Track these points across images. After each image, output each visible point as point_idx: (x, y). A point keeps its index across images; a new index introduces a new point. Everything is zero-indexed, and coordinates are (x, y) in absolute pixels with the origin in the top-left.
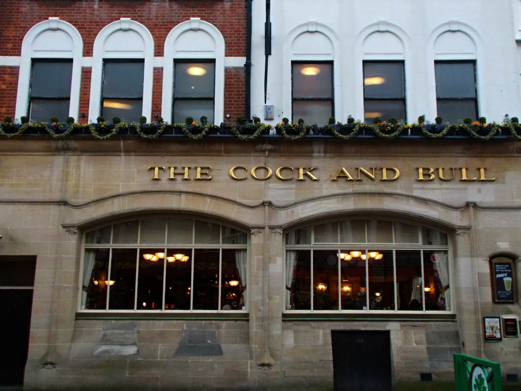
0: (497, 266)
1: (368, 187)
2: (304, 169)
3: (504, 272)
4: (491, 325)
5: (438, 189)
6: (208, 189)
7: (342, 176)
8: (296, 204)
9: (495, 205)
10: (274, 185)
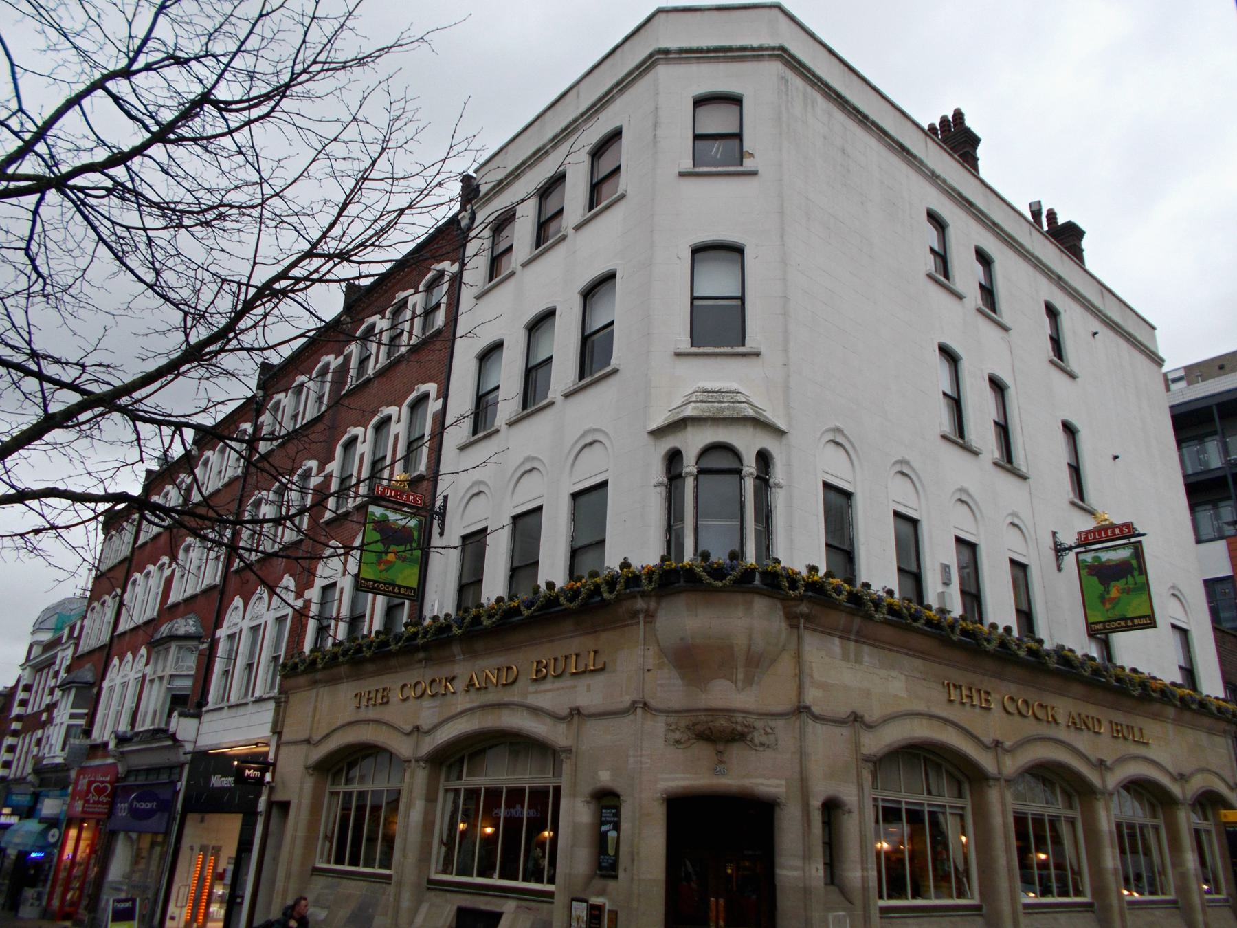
1: (491, 697)
2: (446, 679)
3: (609, 822)
4: (578, 913)
6: (386, 714)
7: (471, 684)
8: (435, 728)
9: (601, 709)
10: (426, 703)
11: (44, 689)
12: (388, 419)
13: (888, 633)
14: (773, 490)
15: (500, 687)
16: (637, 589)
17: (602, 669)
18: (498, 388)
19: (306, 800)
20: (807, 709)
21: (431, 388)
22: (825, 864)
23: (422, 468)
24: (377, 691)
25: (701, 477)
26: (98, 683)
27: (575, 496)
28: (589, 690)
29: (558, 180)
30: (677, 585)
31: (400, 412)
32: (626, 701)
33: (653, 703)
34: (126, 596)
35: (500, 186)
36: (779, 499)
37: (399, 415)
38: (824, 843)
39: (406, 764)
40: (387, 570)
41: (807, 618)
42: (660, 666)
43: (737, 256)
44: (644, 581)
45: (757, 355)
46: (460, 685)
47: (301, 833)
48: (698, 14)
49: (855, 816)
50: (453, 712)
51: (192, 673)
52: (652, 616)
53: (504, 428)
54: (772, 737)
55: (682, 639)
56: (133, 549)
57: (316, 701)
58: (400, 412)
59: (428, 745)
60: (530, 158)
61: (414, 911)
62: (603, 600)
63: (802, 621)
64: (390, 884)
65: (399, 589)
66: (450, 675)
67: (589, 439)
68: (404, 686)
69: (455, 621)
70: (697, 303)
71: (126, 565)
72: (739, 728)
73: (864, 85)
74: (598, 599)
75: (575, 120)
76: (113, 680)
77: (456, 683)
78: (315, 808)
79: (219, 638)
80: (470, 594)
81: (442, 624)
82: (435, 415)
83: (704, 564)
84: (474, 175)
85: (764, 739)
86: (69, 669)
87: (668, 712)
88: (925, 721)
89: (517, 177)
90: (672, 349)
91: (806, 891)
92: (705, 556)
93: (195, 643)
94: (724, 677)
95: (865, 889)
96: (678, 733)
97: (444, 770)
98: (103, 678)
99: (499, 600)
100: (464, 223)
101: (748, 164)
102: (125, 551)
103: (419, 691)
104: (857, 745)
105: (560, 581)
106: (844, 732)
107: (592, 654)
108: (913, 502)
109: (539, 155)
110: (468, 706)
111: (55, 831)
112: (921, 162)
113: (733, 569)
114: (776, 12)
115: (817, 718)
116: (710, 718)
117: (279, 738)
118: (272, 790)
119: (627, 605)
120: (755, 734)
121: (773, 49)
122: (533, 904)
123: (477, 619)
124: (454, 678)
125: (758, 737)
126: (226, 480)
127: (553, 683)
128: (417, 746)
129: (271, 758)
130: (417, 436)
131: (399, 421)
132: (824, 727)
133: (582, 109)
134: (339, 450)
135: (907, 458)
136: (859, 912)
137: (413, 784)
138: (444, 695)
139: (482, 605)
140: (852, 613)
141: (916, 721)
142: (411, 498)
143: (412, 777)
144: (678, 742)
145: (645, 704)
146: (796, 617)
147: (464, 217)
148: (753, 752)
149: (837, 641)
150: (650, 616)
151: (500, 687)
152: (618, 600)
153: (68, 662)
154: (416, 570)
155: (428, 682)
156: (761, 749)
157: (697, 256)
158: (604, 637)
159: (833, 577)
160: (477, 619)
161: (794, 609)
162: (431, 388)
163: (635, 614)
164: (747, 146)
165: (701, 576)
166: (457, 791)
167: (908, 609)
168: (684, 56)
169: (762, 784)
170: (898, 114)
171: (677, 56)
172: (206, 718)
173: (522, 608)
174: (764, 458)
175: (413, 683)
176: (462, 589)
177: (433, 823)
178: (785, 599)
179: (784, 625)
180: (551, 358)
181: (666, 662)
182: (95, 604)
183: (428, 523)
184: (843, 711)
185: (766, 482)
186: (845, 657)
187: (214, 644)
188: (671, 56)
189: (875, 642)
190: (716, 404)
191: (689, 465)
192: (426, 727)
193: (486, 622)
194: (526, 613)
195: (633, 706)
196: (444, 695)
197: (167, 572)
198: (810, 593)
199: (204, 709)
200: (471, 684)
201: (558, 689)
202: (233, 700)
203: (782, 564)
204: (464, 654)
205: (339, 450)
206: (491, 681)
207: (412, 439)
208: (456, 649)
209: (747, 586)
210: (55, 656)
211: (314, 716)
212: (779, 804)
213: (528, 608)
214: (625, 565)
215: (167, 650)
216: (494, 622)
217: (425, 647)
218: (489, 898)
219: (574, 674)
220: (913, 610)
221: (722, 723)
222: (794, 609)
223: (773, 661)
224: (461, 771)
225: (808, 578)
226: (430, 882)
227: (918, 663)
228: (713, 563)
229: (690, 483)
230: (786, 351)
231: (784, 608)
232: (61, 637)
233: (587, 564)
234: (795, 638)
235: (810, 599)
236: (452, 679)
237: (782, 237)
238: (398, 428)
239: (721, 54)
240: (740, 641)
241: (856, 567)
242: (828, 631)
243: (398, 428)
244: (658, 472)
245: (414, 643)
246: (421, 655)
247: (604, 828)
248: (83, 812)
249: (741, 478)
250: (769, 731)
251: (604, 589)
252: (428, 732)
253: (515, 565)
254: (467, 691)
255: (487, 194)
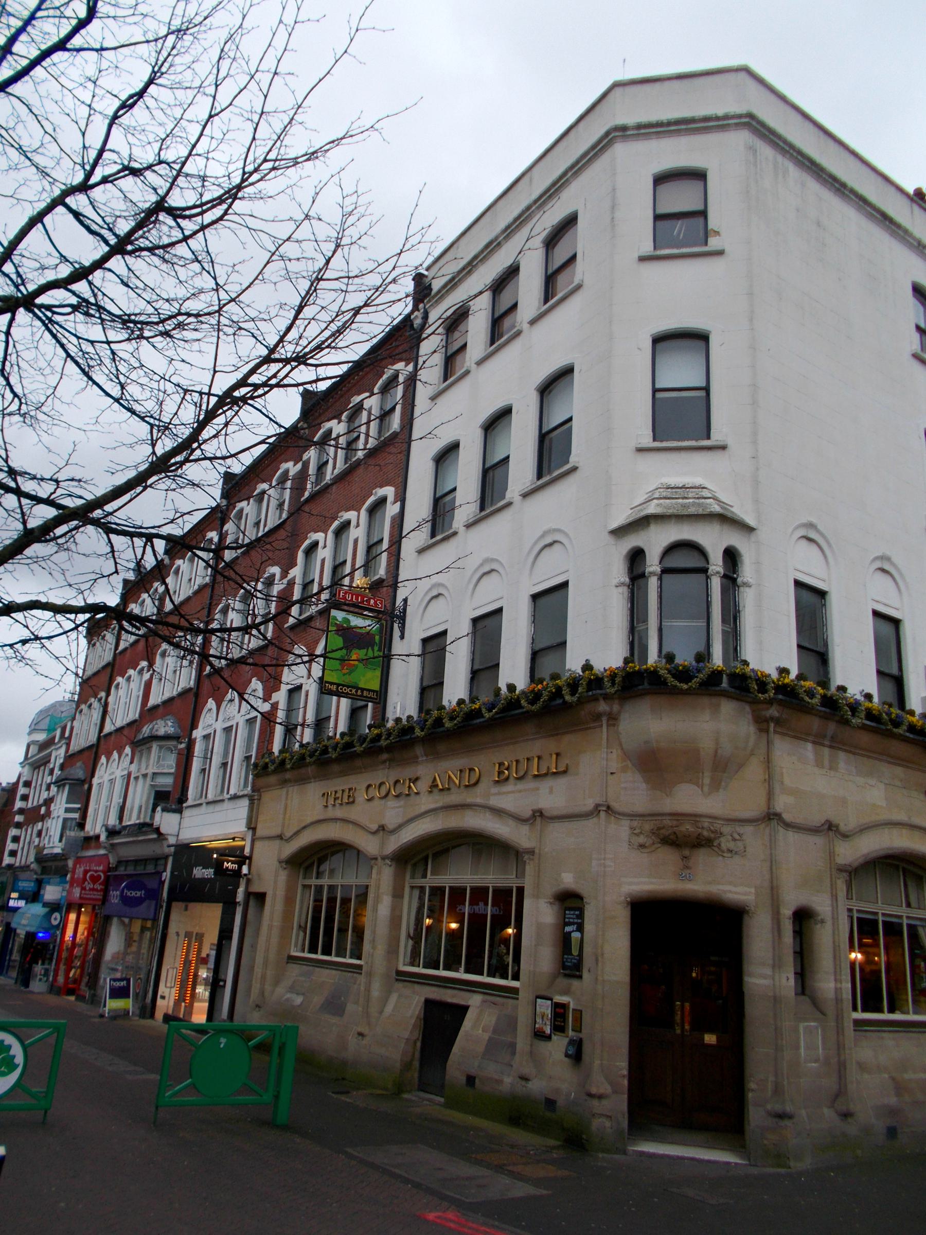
0: (567, 912)
1: (454, 798)
2: (410, 780)
3: (573, 924)
4: (542, 1010)
5: (513, 792)
6: (353, 813)
8: (400, 827)
10: (391, 803)
11: (41, 785)
12: (348, 523)
13: (865, 738)
14: (742, 589)
15: (462, 787)
16: (599, 692)
17: (565, 772)
18: (454, 489)
19: (281, 892)
20: (778, 816)
21: (389, 491)
22: (796, 973)
23: (382, 572)
24: (343, 791)
25: (665, 576)
26: (88, 779)
27: (535, 597)
28: (551, 792)
29: (513, 271)
30: (640, 687)
31: (326, 538)
32: (589, 804)
33: (615, 805)
34: (111, 699)
35: (453, 283)
36: (748, 599)
37: (325, 541)
38: (795, 952)
39: (373, 862)
40: (349, 674)
41: (778, 722)
42: (624, 770)
43: (702, 344)
44: (607, 684)
45: (723, 448)
46: (423, 785)
47: (277, 923)
48: (657, 85)
49: (829, 926)
50: (417, 812)
51: (173, 771)
52: (615, 719)
53: (462, 530)
54: (740, 844)
55: (646, 742)
56: (115, 654)
57: (287, 799)
58: (326, 538)
59: (394, 844)
60: (482, 251)
61: (384, 1001)
62: (565, 702)
63: (772, 725)
64: (361, 974)
65: (362, 692)
66: (413, 776)
67: (548, 540)
68: (369, 786)
69: (418, 722)
70: (659, 395)
71: (109, 669)
72: (705, 833)
73: (841, 149)
74: (560, 701)
75: (528, 208)
76: (101, 777)
77: (419, 783)
78: (289, 900)
79: (195, 739)
80: (430, 695)
81: (404, 726)
82: (393, 519)
83: (668, 666)
84: (426, 273)
85: (731, 845)
86: (62, 767)
87: (632, 816)
88: (904, 831)
89: (470, 273)
90: (633, 444)
91: (776, 1000)
92: (670, 658)
93: (174, 743)
94: (690, 781)
95: (838, 1000)
96: (642, 836)
97: (409, 868)
98: (93, 775)
99: (461, 702)
100: (417, 322)
101: (714, 243)
102: (108, 657)
103: (384, 791)
104: (832, 855)
105: (522, 683)
106: (817, 842)
107: (554, 756)
108: (895, 602)
109: (492, 247)
110: (432, 806)
111: (57, 915)
112: (906, 231)
113: (699, 671)
114: (743, 75)
115: (788, 825)
116: (675, 823)
117: (254, 834)
118: (249, 882)
119: (589, 707)
120: (723, 840)
121: (740, 116)
122: (498, 999)
123: (439, 722)
124: (417, 779)
125: (725, 843)
126: (196, 587)
127: (516, 784)
128: (383, 844)
129: (247, 851)
130: (376, 540)
131: (358, 525)
132: (797, 836)
133: (535, 196)
134: (300, 556)
135: (888, 553)
136: (833, 1024)
137: (379, 880)
138: (408, 795)
139: (443, 708)
140: (825, 717)
141: (895, 832)
142: (372, 602)
143: (379, 873)
144: (642, 846)
145: (609, 807)
146: (767, 720)
147: (416, 316)
148: (721, 858)
149: (809, 746)
150: (613, 719)
151: (462, 787)
152: (580, 702)
153: (62, 761)
154: (378, 673)
155: (392, 783)
156: (729, 855)
157: (659, 346)
158: (567, 739)
159: (805, 679)
160: (439, 722)
161: (763, 713)
162: (389, 491)
163: (598, 717)
164: (712, 223)
165: (665, 679)
166: (422, 889)
167: (889, 714)
168: (643, 131)
169: (730, 892)
170: (880, 179)
171: (635, 132)
172: (186, 813)
173: (484, 710)
174: (731, 556)
175: (377, 784)
176: (423, 691)
177: (400, 918)
178: (754, 702)
179: (752, 729)
180: (508, 457)
181: (630, 765)
182: (83, 706)
183: (389, 626)
184: (817, 819)
185: (734, 581)
186: (819, 764)
187: (191, 744)
188: (629, 133)
189: (852, 749)
190: (680, 501)
191: (653, 564)
192: (391, 827)
193: (448, 724)
194: (487, 715)
195: (596, 810)
196: (408, 795)
197: (146, 676)
198: (780, 697)
199: (184, 805)
200: (434, 785)
201: (520, 791)
202: (210, 797)
203: (751, 667)
204: (426, 755)
205: (300, 556)
206: (454, 781)
207: (371, 543)
208: (419, 750)
209: (713, 688)
210: (50, 755)
211: (285, 813)
212: (747, 912)
213: (490, 710)
214: (587, 667)
215: (150, 749)
216: (456, 725)
217: (389, 749)
218: (456, 992)
219: (535, 776)
220: (893, 716)
221: (687, 828)
222: (763, 713)
223: (741, 766)
224: (426, 870)
225: (778, 680)
226: (399, 973)
227: (899, 771)
228: (678, 665)
229: (653, 583)
230: (755, 442)
231: (753, 711)
232: (54, 737)
233: (547, 667)
234: (764, 742)
235: (780, 703)
236: (415, 780)
237: (751, 320)
238: (357, 533)
239: (683, 127)
240: (706, 745)
241: (831, 669)
242: (800, 736)
243: (357, 533)
244: (619, 572)
245: (379, 744)
246: (385, 756)
247: (568, 929)
248: (81, 898)
249: (708, 577)
250: (737, 837)
251: (565, 691)
252: (393, 831)
253: (476, 667)
254: (430, 792)
255: (439, 291)
